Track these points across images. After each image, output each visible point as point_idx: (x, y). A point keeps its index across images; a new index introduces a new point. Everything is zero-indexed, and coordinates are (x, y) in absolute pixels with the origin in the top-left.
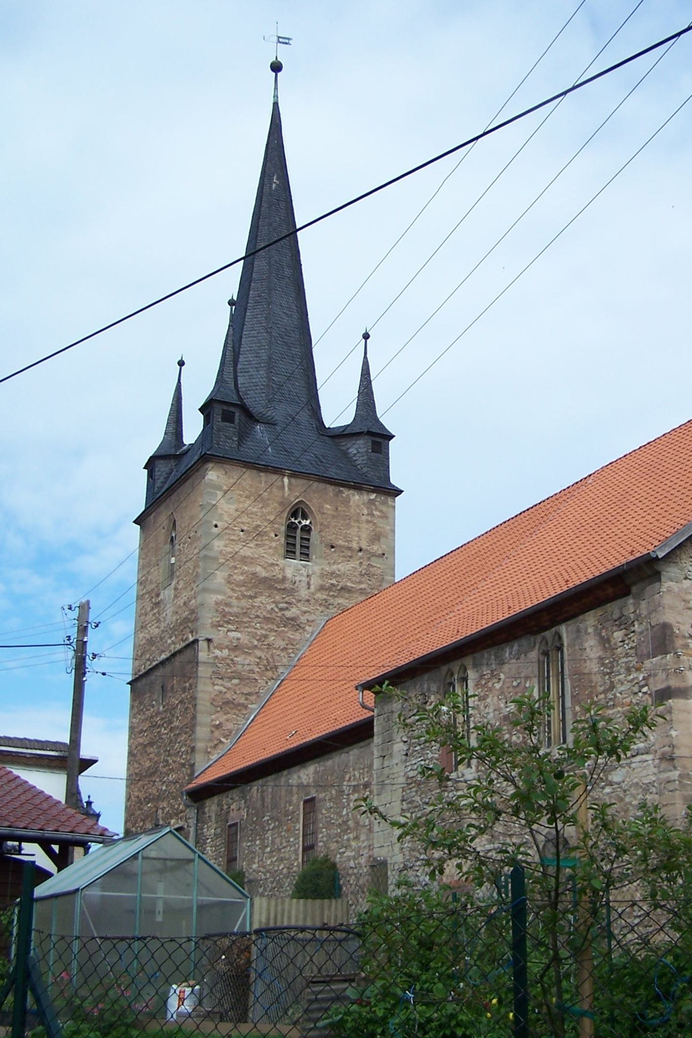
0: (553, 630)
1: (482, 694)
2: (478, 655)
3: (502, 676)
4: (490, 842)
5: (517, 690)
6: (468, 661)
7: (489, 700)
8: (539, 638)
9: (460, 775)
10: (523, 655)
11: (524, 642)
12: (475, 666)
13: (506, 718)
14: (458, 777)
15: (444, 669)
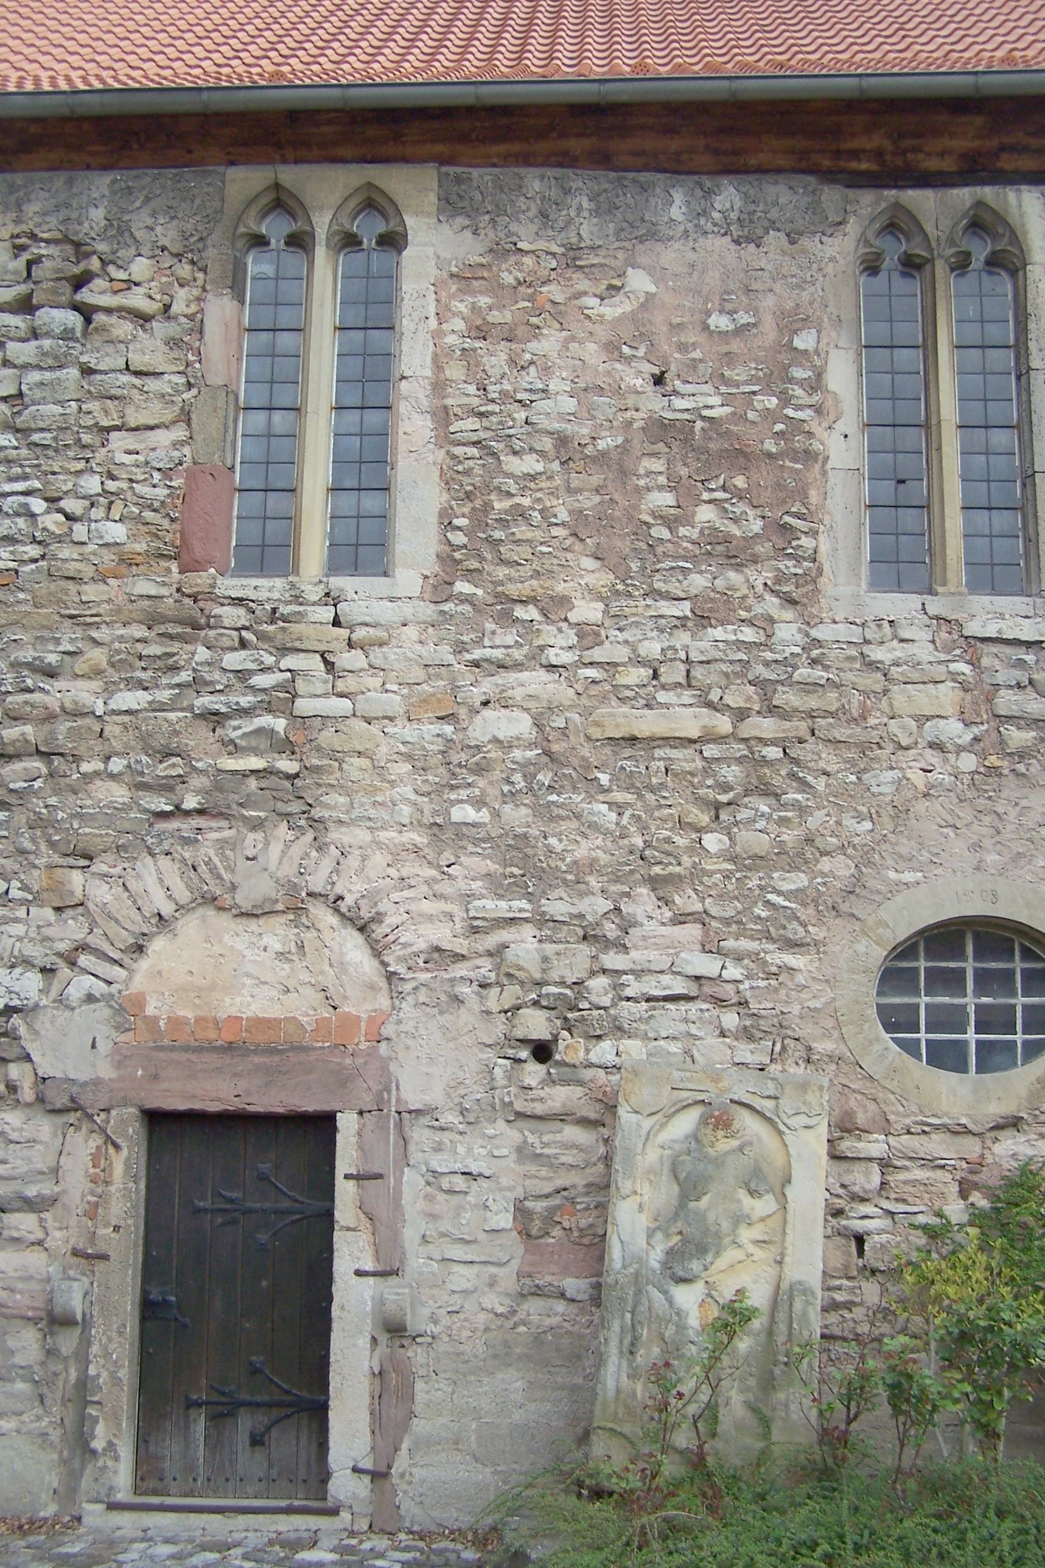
0: (964, 196)
1: (495, 317)
2: (481, 176)
3: (639, 282)
4: (498, 887)
5: (736, 345)
6: (413, 188)
7: (549, 343)
8: (869, 203)
9: (314, 594)
10: (775, 240)
11: (783, 196)
12: (450, 205)
13: (662, 430)
14: (298, 599)
15: (245, 181)
